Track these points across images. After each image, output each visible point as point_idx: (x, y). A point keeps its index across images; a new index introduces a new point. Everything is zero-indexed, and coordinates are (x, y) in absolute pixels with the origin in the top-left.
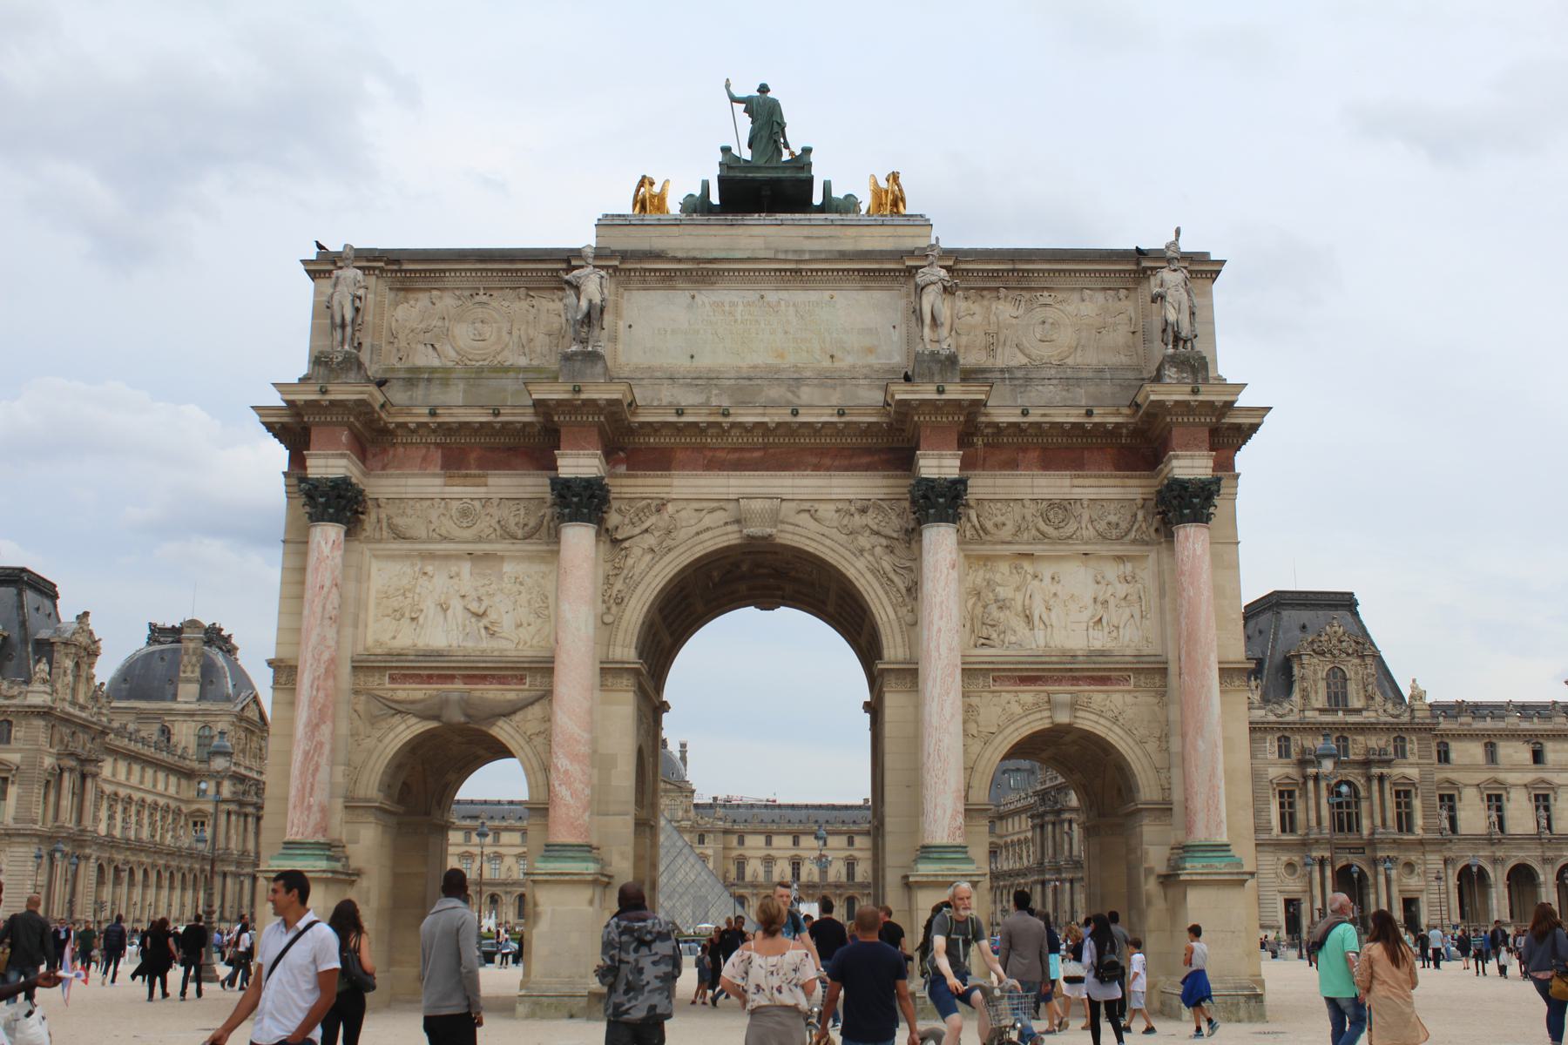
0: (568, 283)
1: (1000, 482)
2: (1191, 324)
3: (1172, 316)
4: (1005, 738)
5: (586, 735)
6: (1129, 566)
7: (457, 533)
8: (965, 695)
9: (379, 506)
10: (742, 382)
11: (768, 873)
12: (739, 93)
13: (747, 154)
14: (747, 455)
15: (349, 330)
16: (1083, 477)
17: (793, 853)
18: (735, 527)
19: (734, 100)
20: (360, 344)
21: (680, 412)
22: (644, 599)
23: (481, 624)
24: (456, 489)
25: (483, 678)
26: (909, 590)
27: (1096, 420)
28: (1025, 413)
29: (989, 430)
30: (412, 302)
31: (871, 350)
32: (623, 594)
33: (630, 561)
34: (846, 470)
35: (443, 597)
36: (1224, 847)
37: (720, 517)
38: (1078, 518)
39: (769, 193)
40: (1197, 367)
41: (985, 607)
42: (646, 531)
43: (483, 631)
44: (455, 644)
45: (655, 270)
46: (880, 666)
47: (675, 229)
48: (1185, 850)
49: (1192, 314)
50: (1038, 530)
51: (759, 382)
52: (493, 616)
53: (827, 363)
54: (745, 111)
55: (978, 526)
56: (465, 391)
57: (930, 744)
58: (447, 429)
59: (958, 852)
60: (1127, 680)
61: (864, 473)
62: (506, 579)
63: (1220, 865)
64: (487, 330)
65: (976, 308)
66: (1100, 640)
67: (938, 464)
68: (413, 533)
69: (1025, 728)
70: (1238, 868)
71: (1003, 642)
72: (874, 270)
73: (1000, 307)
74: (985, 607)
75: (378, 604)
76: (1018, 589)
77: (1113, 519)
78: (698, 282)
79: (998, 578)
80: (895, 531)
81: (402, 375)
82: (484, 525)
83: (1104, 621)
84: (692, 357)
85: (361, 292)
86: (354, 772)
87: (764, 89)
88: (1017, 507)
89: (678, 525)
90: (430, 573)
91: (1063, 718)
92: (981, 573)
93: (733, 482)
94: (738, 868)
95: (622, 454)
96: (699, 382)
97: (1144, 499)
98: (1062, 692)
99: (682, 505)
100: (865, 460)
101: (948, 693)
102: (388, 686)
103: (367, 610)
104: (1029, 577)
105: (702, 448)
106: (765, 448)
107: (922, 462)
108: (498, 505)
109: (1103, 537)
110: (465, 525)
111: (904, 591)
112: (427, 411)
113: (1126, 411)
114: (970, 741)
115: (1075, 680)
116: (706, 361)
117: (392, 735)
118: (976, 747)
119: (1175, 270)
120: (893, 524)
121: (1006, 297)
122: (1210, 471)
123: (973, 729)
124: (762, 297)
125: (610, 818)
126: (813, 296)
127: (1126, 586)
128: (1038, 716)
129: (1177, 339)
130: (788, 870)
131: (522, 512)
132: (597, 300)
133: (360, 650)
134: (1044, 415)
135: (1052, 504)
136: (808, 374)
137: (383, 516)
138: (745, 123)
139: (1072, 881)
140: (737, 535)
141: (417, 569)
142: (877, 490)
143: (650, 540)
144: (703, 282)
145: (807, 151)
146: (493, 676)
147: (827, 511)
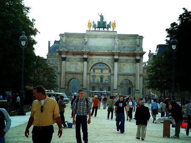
8: (118, 76)
11: (94, 80)
13: (100, 21)
17: (101, 74)
31: (111, 45)
36: (138, 90)
48: (136, 90)
53: (107, 46)
57: (114, 81)
59: (117, 90)
63: (138, 92)
65: (121, 41)
86: (66, 82)
87: (102, 14)
91: (126, 78)
98: (126, 76)
109: (130, 63)
115: (128, 75)
116: (96, 45)
120: (113, 61)
130: (99, 79)
138: (100, 18)
143: (91, 62)
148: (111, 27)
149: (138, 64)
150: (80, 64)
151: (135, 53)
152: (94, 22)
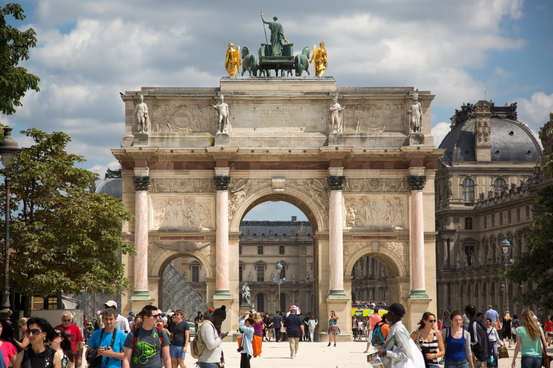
0: (215, 108)
2: (421, 122)
3: (414, 120)
6: (398, 200)
7: (179, 190)
9: (154, 182)
10: (272, 139)
12: (265, 21)
13: (270, 44)
14: (274, 164)
15: (144, 125)
18: (270, 188)
19: (264, 22)
20: (147, 129)
21: (253, 151)
23: (189, 220)
24: (179, 176)
25: (191, 238)
26: (326, 209)
27: (388, 153)
29: (353, 156)
30: (159, 109)
32: (235, 210)
33: (237, 200)
34: (306, 169)
35: (176, 211)
37: (265, 184)
38: (382, 185)
40: (420, 139)
41: (351, 213)
43: (190, 223)
44: (180, 226)
45: (242, 100)
46: (317, 233)
49: (421, 118)
50: (368, 189)
51: (277, 139)
52: (192, 217)
54: (269, 28)
55: (349, 187)
56: (180, 142)
58: (176, 157)
60: (396, 237)
61: (312, 170)
62: (196, 205)
64: (185, 118)
66: (388, 224)
67: (337, 172)
68: (167, 191)
72: (316, 100)
73: (358, 111)
74: (351, 213)
75: (154, 214)
76: (362, 207)
77: (393, 184)
79: (355, 204)
80: (322, 189)
81: (158, 136)
82: (189, 188)
83: (390, 218)
85: (147, 112)
88: (362, 181)
92: (350, 202)
93: (269, 173)
94: (193, 271)
95: (233, 164)
96: (258, 139)
97: (404, 178)
99: (253, 181)
100: (312, 165)
102: (160, 241)
104: (365, 204)
105: (259, 162)
106: (280, 162)
107: (331, 171)
108: (193, 181)
109: (389, 191)
110: (182, 188)
111: (325, 209)
112: (170, 151)
113: (398, 150)
114: (346, 257)
117: (162, 256)
118: (347, 259)
119: (416, 104)
121: (360, 108)
122: (423, 173)
123: (347, 253)
124: (278, 108)
126: (295, 107)
127: (397, 207)
128: (367, 249)
129: (415, 129)
131: (201, 183)
132: (226, 115)
133: (151, 229)
134: (371, 152)
135: (373, 179)
136: (293, 136)
137: (155, 185)
138: (269, 32)
139: (449, 284)
140: (271, 191)
141: (167, 201)
142: (316, 176)
143: (243, 193)
145: (292, 45)
146: (194, 237)
147: (300, 182)
148: (312, 67)
149: (420, 195)
150: (201, 199)
151: (404, 155)
152: (245, 51)
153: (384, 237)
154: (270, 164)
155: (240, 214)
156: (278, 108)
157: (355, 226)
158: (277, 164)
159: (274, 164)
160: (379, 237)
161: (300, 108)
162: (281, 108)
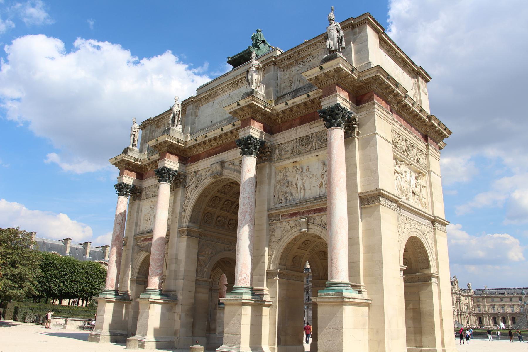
1: (286, 135)
4: (284, 241)
5: (157, 252)
16: (314, 124)
22: (191, 205)
27: (312, 98)
28: (287, 104)
39: (243, 61)
42: (193, 183)
47: (213, 83)
69: (291, 236)
70: (340, 295)
71: (287, 200)
78: (213, 97)
84: (212, 122)
89: (201, 179)
90: (153, 208)
95: (190, 159)
101: (242, 223)
103: (140, 221)
106: (222, 145)
117: (140, 258)
123: (273, 239)
124: (229, 95)
125: (179, 281)
134: (293, 103)
144: (215, 97)
153: (314, 210)
154: (214, 150)
155: (190, 208)
156: (229, 95)
157: (284, 201)
158: (220, 148)
159: (217, 149)
160: (310, 212)
161: (246, 88)
162: (231, 94)
